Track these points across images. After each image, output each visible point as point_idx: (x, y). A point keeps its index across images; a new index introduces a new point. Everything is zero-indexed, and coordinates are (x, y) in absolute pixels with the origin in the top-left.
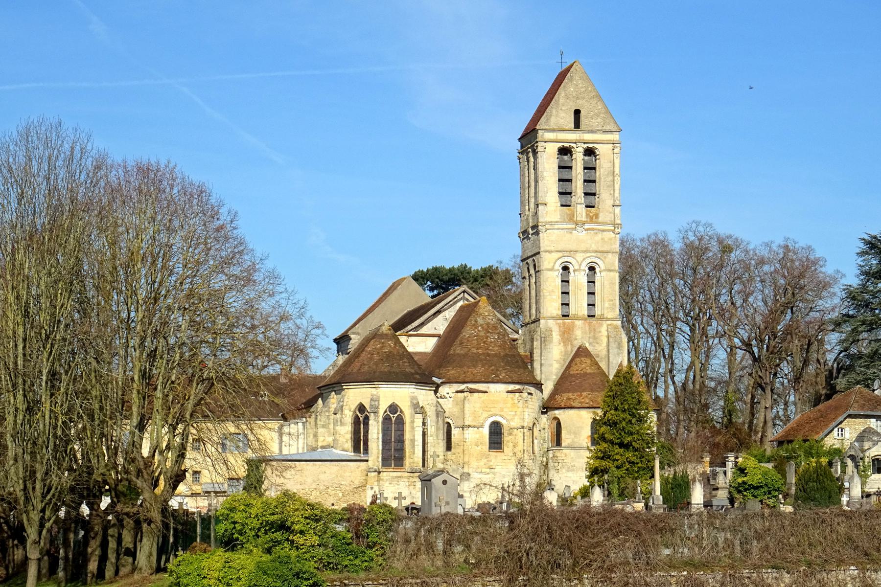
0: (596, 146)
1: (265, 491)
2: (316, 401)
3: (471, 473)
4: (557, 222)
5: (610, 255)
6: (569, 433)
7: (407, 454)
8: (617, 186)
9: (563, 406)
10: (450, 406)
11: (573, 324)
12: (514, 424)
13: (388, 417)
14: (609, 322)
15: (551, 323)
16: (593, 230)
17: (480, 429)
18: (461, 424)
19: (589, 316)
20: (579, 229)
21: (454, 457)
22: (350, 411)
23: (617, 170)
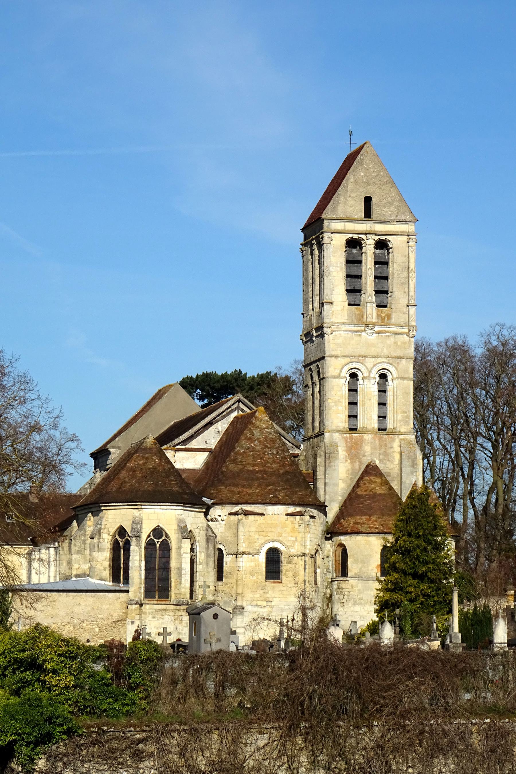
0: (388, 238)
1: (12, 624)
2: (71, 523)
3: (245, 607)
4: (344, 323)
5: (404, 361)
6: (356, 561)
7: (173, 584)
8: (412, 284)
9: (349, 531)
10: (222, 530)
11: (362, 439)
12: (293, 551)
13: (151, 542)
14: (402, 437)
15: (337, 436)
16: (384, 332)
17: (256, 556)
18: (233, 550)
19: (379, 430)
20: (368, 331)
21: (226, 588)
22: (109, 534)
23: (412, 266)
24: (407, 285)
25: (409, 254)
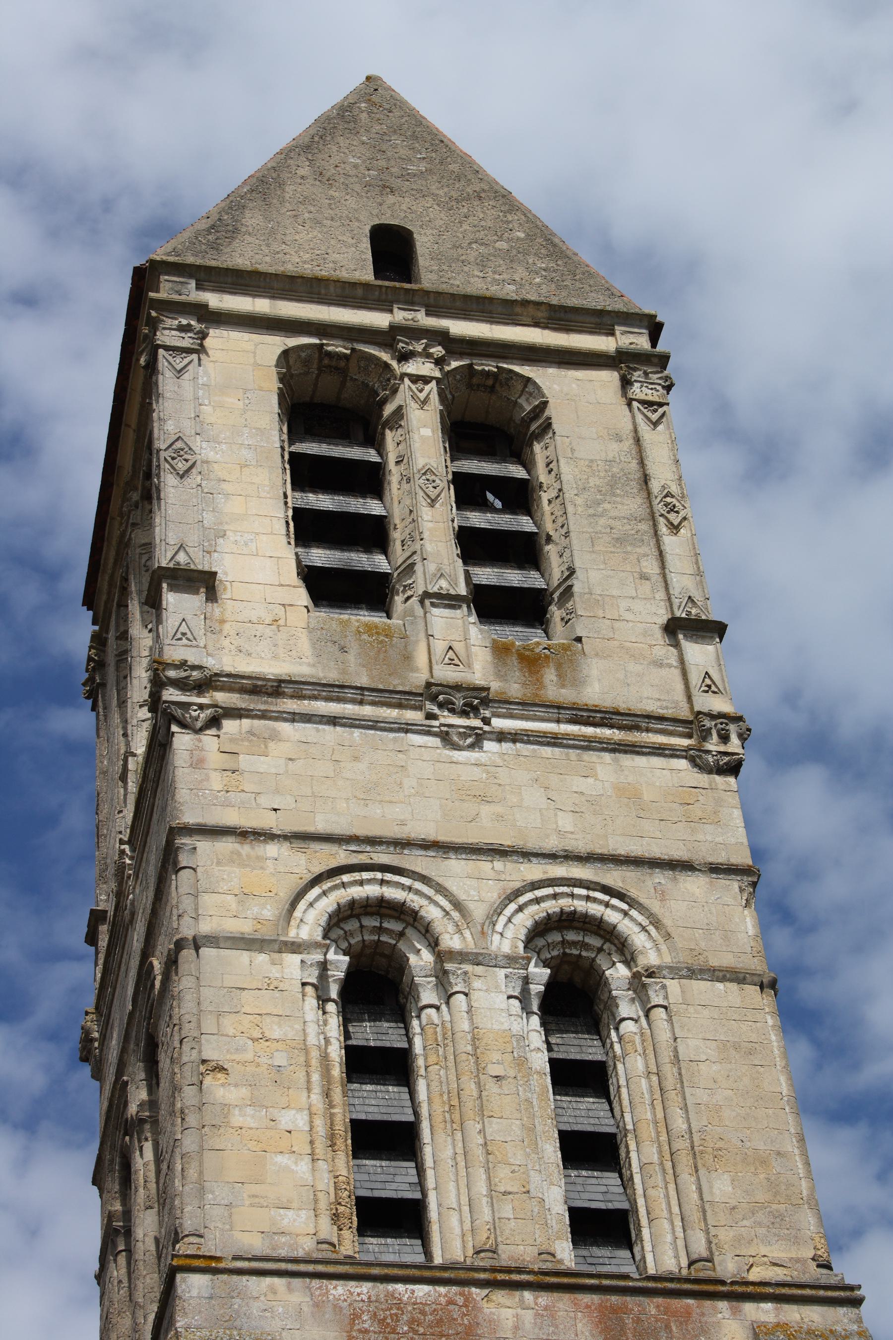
24: (649, 549)
25: (636, 431)
